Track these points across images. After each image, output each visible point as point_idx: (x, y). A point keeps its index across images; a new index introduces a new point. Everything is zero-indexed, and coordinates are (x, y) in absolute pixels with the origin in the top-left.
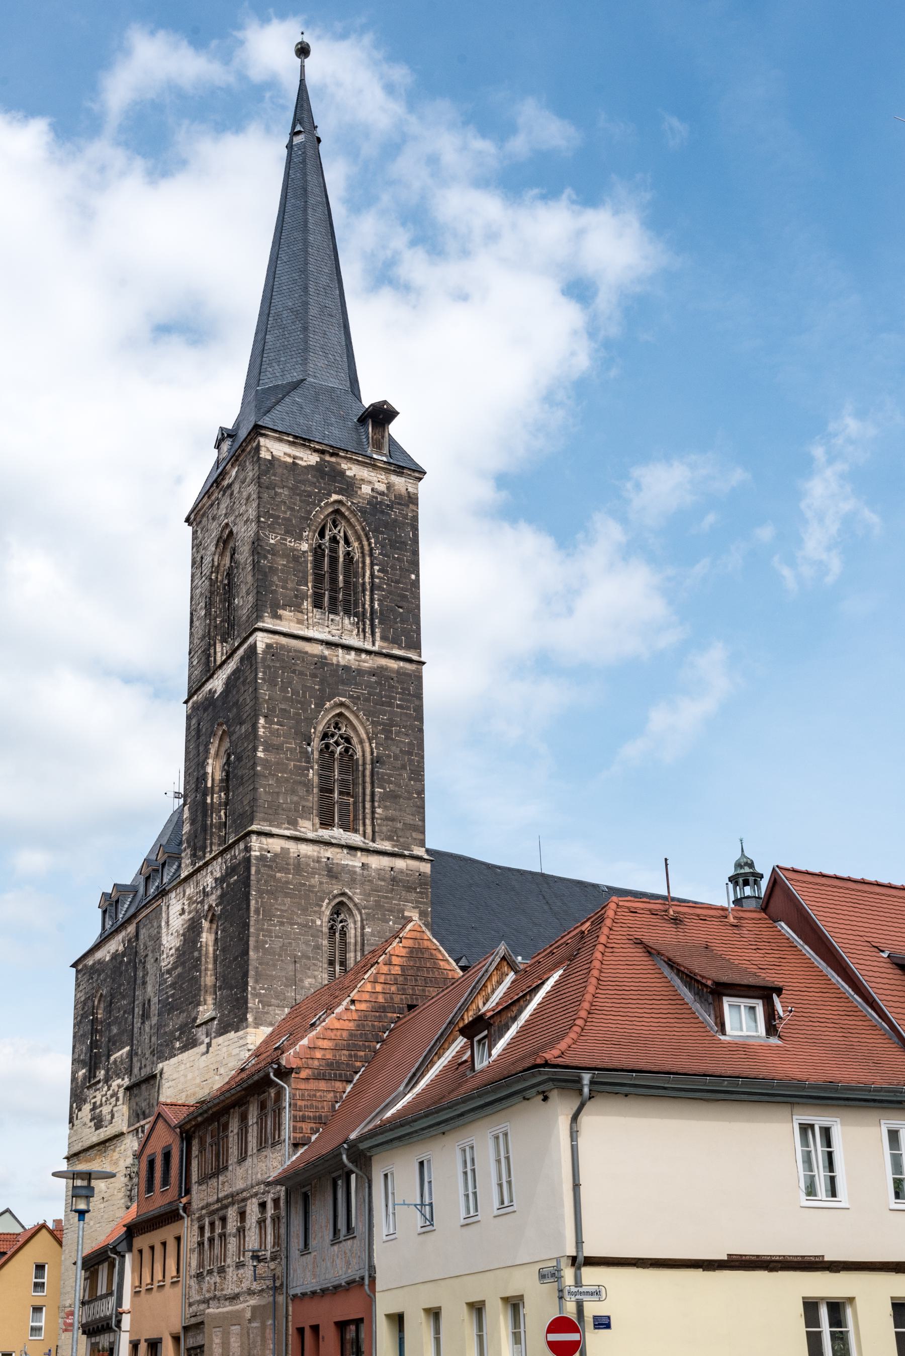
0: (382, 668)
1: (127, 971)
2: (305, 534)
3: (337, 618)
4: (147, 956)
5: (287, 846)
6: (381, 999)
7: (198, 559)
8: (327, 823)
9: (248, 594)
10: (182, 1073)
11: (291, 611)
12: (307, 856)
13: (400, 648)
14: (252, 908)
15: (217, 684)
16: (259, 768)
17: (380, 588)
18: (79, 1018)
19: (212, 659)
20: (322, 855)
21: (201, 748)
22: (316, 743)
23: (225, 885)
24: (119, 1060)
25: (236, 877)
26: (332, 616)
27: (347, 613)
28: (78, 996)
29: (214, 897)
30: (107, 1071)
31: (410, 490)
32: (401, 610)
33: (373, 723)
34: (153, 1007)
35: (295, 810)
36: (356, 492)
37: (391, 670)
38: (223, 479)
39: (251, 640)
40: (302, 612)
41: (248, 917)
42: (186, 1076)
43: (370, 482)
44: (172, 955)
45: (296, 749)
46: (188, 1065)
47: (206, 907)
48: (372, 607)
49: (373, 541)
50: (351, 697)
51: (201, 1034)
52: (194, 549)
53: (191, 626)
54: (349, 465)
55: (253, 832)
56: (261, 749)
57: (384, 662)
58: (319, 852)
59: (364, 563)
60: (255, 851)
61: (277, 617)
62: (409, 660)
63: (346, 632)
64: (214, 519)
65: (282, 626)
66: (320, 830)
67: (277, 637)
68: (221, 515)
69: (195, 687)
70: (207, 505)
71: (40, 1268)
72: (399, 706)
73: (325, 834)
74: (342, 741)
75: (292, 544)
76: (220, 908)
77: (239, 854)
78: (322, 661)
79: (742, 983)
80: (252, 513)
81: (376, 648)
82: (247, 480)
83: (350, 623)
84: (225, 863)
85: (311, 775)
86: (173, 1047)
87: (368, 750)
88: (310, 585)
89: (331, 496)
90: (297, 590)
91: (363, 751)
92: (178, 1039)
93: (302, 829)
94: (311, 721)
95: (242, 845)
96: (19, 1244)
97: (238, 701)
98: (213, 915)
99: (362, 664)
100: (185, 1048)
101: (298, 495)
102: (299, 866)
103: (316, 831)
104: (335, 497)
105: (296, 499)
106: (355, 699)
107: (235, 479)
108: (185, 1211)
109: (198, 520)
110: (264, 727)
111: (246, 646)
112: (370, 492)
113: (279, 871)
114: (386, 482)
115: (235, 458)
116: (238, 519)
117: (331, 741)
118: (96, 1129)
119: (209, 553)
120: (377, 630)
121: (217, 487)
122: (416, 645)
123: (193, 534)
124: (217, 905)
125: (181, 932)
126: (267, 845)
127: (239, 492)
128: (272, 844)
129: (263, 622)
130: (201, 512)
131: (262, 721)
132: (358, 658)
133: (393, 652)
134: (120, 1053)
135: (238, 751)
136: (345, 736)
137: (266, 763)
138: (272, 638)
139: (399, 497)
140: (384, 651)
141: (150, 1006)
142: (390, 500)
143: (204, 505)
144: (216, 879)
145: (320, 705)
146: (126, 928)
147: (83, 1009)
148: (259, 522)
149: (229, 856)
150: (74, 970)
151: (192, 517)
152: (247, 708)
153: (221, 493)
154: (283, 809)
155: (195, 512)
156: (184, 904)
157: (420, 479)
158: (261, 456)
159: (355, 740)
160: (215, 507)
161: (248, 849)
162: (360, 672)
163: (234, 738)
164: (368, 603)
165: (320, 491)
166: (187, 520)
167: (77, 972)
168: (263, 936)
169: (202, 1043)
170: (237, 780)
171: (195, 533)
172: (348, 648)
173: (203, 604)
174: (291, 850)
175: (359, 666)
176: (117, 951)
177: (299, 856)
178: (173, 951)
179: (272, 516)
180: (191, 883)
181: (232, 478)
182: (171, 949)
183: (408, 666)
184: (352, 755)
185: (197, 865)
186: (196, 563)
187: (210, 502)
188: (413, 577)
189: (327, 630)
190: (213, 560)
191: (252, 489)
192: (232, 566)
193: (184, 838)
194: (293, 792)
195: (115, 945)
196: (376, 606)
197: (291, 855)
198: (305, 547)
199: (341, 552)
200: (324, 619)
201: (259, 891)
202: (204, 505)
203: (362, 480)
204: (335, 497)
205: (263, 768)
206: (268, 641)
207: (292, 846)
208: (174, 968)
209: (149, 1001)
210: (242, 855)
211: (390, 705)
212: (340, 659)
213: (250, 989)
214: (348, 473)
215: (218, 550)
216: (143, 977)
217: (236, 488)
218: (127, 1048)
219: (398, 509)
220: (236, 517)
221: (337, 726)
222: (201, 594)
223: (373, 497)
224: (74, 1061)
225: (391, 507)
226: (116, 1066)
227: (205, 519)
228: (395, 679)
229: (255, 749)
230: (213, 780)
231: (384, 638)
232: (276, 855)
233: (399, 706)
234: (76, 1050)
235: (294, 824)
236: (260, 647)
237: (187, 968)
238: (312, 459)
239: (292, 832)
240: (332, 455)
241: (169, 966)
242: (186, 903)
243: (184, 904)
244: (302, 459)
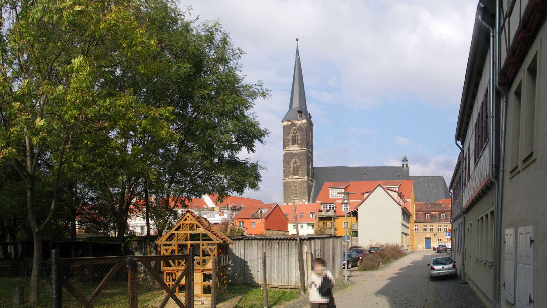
8: (295, 176)
22: (292, 165)
57: (301, 151)
61: (285, 148)
78: (292, 153)
94: (291, 162)
102: (289, 183)
106: (296, 157)
162: (297, 153)
198: (289, 137)
207: (288, 180)
231: (301, 147)
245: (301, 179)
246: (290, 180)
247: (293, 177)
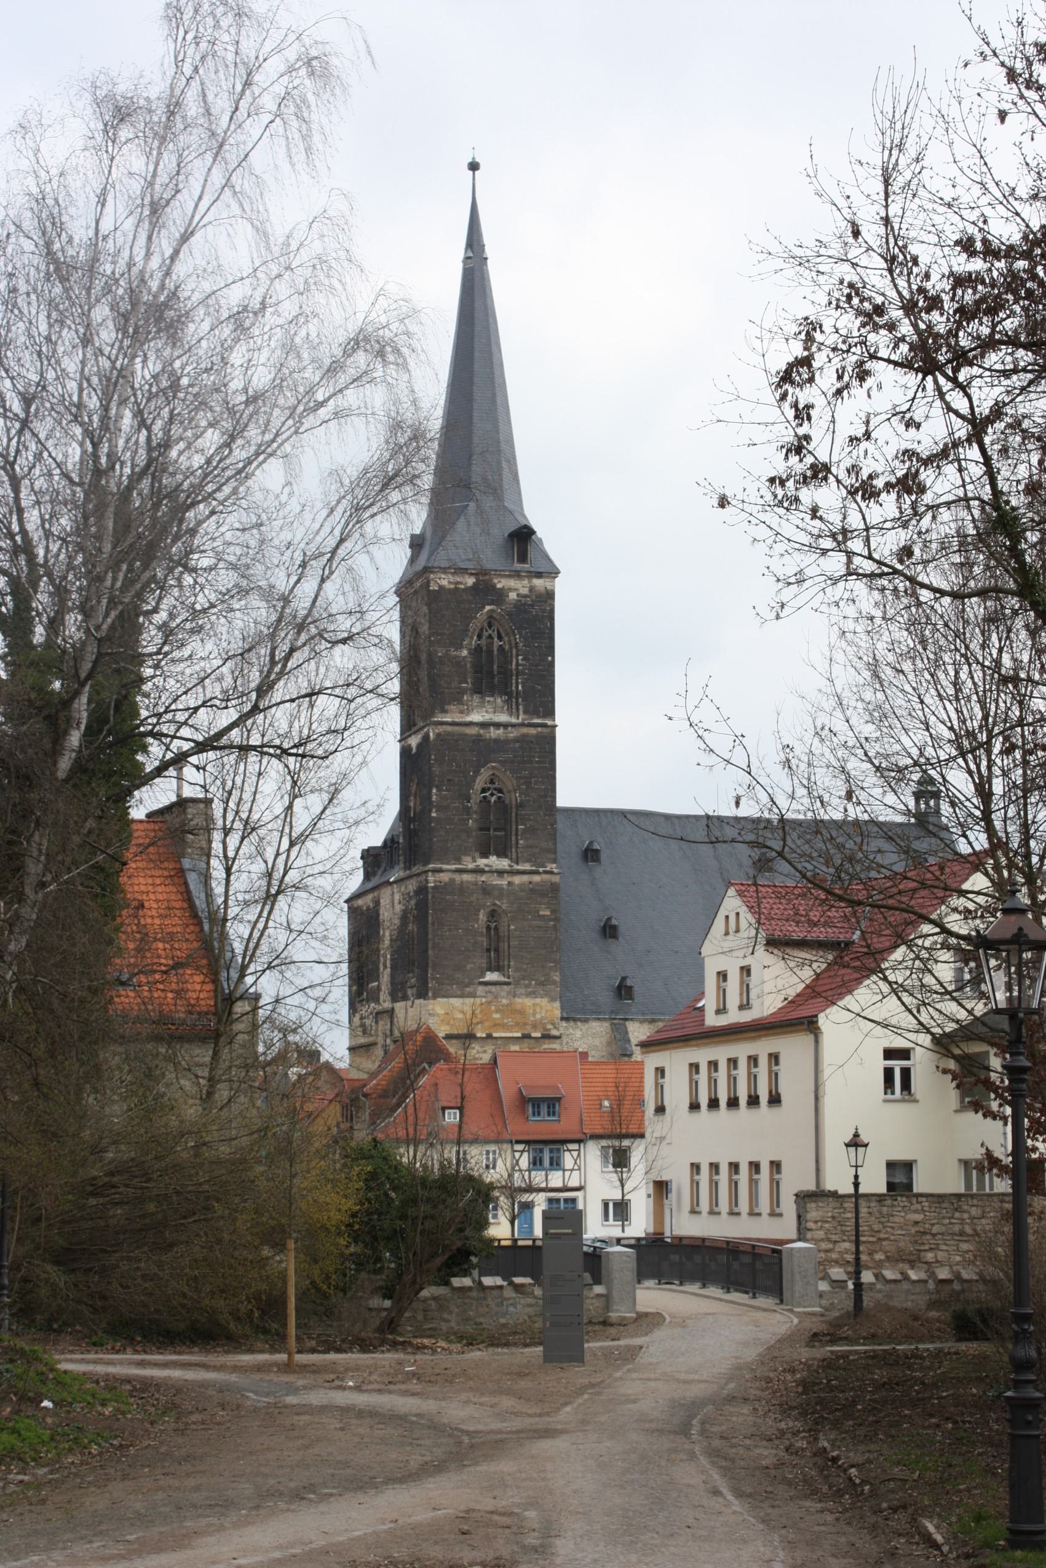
0: (524, 736)
8: (485, 855)
13: (539, 717)
17: (524, 673)
22: (474, 803)
27: (501, 694)
33: (518, 778)
37: (532, 736)
50: (499, 762)
57: (525, 730)
61: (444, 711)
62: (545, 726)
78: (478, 740)
79: (706, 942)
94: (470, 784)
102: (462, 889)
104: (488, 608)
122: (550, 712)
137: (437, 819)
145: (477, 773)
162: (507, 741)
172: (497, 725)
183: (545, 730)
204: (488, 608)
207: (458, 877)
214: (499, 586)
225: (532, 606)
229: (430, 811)
231: (525, 712)
235: (458, 860)
238: (470, 581)
245: (525, 878)
246: (466, 877)
247: (482, 862)
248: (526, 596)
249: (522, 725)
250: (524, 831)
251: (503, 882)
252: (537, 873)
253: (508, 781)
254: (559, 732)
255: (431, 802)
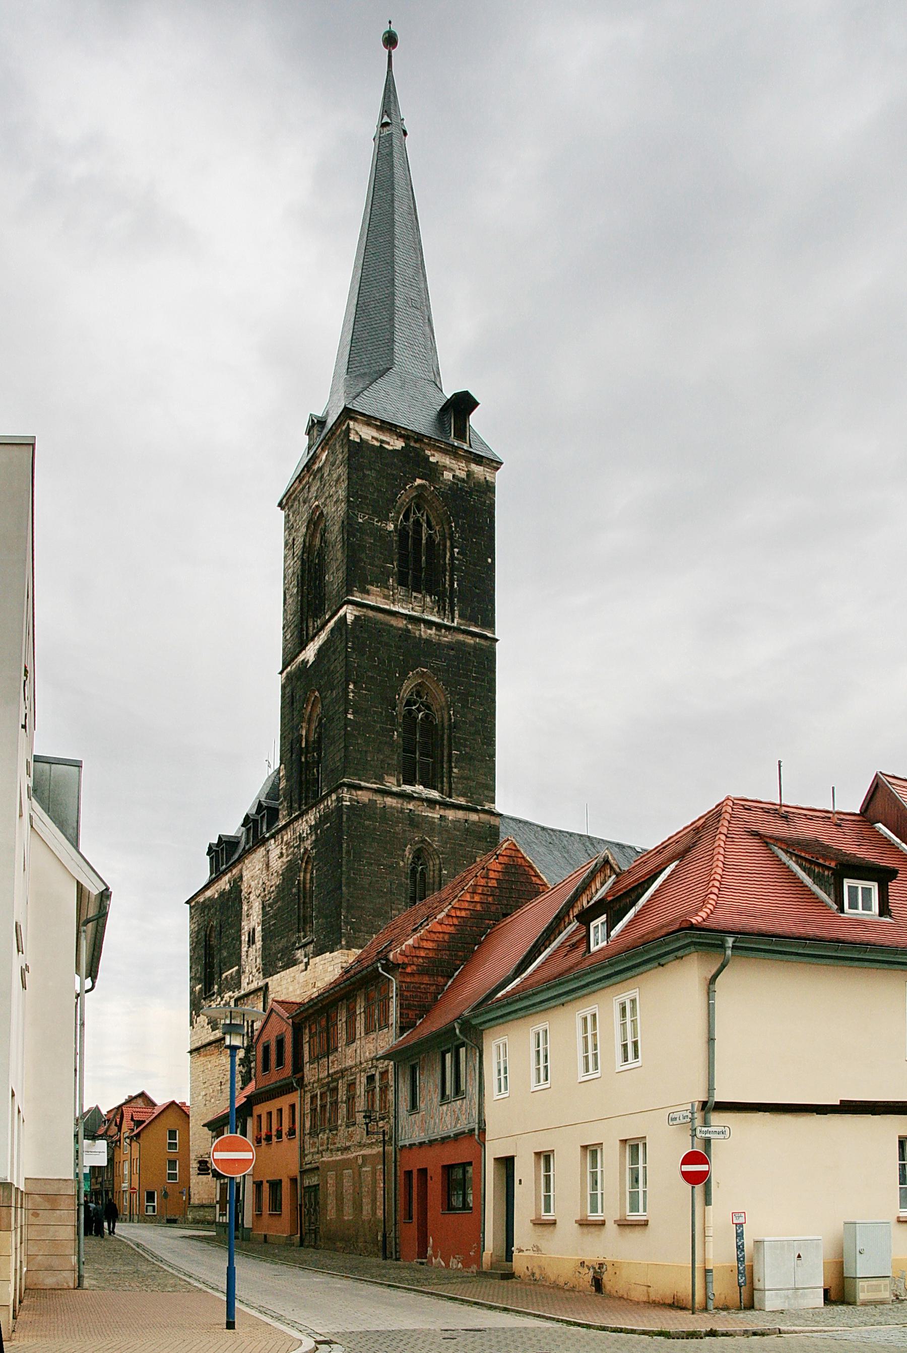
0: (459, 642)
1: (233, 905)
2: (390, 515)
3: (420, 596)
4: (250, 893)
5: (374, 798)
6: (478, 907)
7: (290, 541)
9: (338, 570)
10: (284, 986)
11: (377, 587)
12: (391, 807)
13: (476, 626)
14: (344, 851)
15: (310, 653)
16: (349, 729)
18: (194, 945)
19: (305, 632)
20: (405, 807)
21: (296, 713)
22: (401, 709)
23: (319, 831)
24: (229, 977)
25: (329, 824)
26: (414, 594)
28: (192, 927)
29: (309, 842)
30: (220, 987)
31: (488, 478)
32: (477, 591)
33: (451, 693)
34: (257, 935)
35: (382, 768)
36: (439, 478)
37: (469, 645)
38: (314, 463)
39: (341, 612)
40: (388, 588)
41: (342, 858)
42: (288, 989)
43: (451, 470)
44: (273, 892)
45: (381, 713)
46: (289, 980)
47: (302, 850)
48: (452, 585)
49: (453, 524)
51: (299, 954)
52: (287, 532)
53: (285, 603)
54: (433, 452)
55: (344, 784)
56: (350, 711)
57: (461, 637)
58: (402, 804)
59: (445, 546)
60: (346, 801)
62: (486, 638)
63: (428, 609)
64: (305, 502)
65: (369, 600)
66: (403, 786)
67: (365, 610)
68: (311, 498)
69: (288, 659)
70: (299, 489)
71: (172, 1135)
72: (475, 679)
73: (408, 788)
74: (423, 708)
75: (379, 524)
76: (314, 851)
77: (331, 804)
80: (342, 494)
81: (455, 624)
82: (337, 462)
83: (431, 601)
84: (319, 812)
85: (395, 736)
86: (276, 966)
87: (446, 716)
88: (395, 564)
89: (415, 481)
90: (384, 567)
91: (442, 718)
92: (280, 960)
93: (388, 784)
95: (334, 797)
96: (154, 1115)
97: (329, 668)
98: (309, 857)
99: (441, 638)
100: (286, 967)
101: (384, 477)
103: (400, 786)
104: (419, 481)
105: (383, 482)
106: (435, 671)
107: (325, 462)
108: (299, 1086)
109: (290, 504)
110: (353, 692)
111: (336, 618)
112: (451, 479)
113: (368, 819)
114: (466, 469)
115: (325, 444)
116: (328, 500)
117: (414, 708)
118: (213, 1031)
119: (300, 534)
120: (456, 608)
121: (308, 471)
122: (490, 623)
123: (285, 517)
124: (312, 849)
125: (280, 872)
126: (356, 796)
127: (328, 475)
128: (361, 796)
129: (353, 596)
130: (293, 497)
131: (351, 686)
132: (437, 633)
133: (471, 629)
134: (230, 971)
135: (330, 714)
136: (425, 703)
138: (360, 611)
139: (478, 484)
140: (462, 627)
141: (254, 934)
142: (469, 487)
143: (296, 489)
144: (311, 827)
145: (404, 675)
146: (231, 871)
147: (197, 937)
148: (348, 501)
149: (322, 806)
150: (188, 906)
151: (284, 501)
152: (338, 675)
153: (312, 477)
154: (371, 766)
155: (287, 496)
156: (282, 849)
157: (498, 469)
158: (350, 438)
159: (434, 708)
160: (306, 491)
161: (340, 800)
162: (439, 644)
163: (326, 701)
164: (447, 582)
165: (405, 475)
166: (280, 505)
167: (191, 908)
168: (354, 873)
169: (301, 962)
170: (329, 739)
171: (287, 516)
172: (429, 624)
173: (295, 582)
174: (378, 802)
175: (439, 640)
176: (224, 889)
177: (384, 807)
178: (273, 888)
179: (361, 496)
180: (289, 831)
181: (323, 461)
182: (271, 887)
183: (483, 642)
184: (431, 722)
185: (293, 816)
186: (289, 545)
187: (301, 486)
188: (490, 560)
189: (411, 606)
190: (304, 541)
191: (342, 471)
192: (322, 547)
193: (281, 793)
194: (380, 751)
195: (224, 884)
196: (456, 586)
197: (378, 806)
198: (391, 527)
199: (424, 535)
200: (408, 596)
201: (349, 835)
202: (296, 489)
203: (444, 466)
204: (419, 481)
205: (352, 729)
206: (357, 614)
207: (378, 798)
208: (276, 901)
209: (254, 930)
210: (334, 805)
211: (467, 677)
212: (422, 633)
213: (342, 917)
214: (432, 459)
215: (309, 531)
216: (248, 910)
217: (326, 471)
218: (237, 968)
219: (477, 496)
220: (326, 498)
221: (419, 695)
222: (293, 574)
223: (454, 483)
224: (191, 978)
226: (227, 982)
227: (297, 503)
228: (472, 653)
230: (307, 741)
231: (461, 616)
232: (365, 805)
233: (475, 679)
234: (193, 970)
235: (381, 780)
236: (350, 618)
237: (286, 902)
239: (378, 786)
240: (416, 442)
241: (271, 901)
242: (284, 848)
243: (282, 849)
244: (388, 443)
246: (390, 801)
247: (408, 788)
248: (463, 480)
249: (457, 630)
250: (460, 759)
251: (435, 815)
252: (475, 811)
253: (439, 695)
254: (500, 649)
255: (347, 700)
